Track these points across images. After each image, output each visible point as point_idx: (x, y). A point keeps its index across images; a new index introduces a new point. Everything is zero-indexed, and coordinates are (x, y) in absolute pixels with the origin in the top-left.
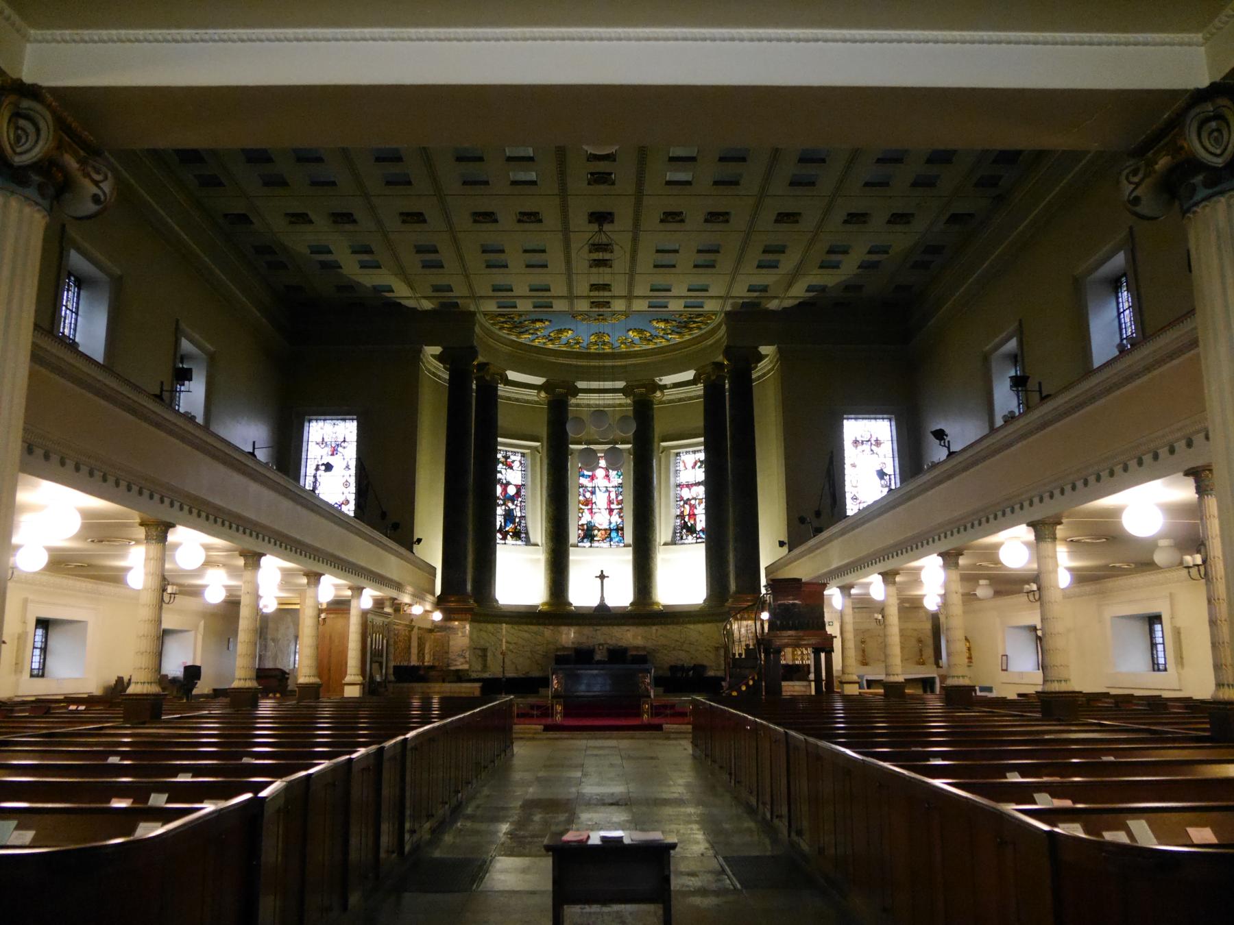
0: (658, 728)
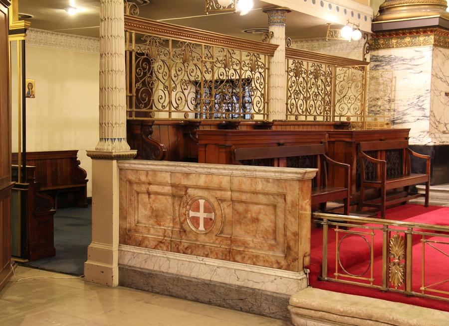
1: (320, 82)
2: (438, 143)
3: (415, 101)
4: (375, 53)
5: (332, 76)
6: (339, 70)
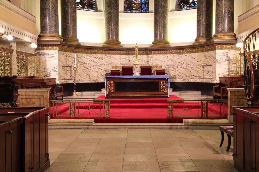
0: (181, 121)
1: (24, 62)
2: (61, 83)
3: (53, 69)
4: (38, 51)
5: (27, 59)
6: (29, 58)
